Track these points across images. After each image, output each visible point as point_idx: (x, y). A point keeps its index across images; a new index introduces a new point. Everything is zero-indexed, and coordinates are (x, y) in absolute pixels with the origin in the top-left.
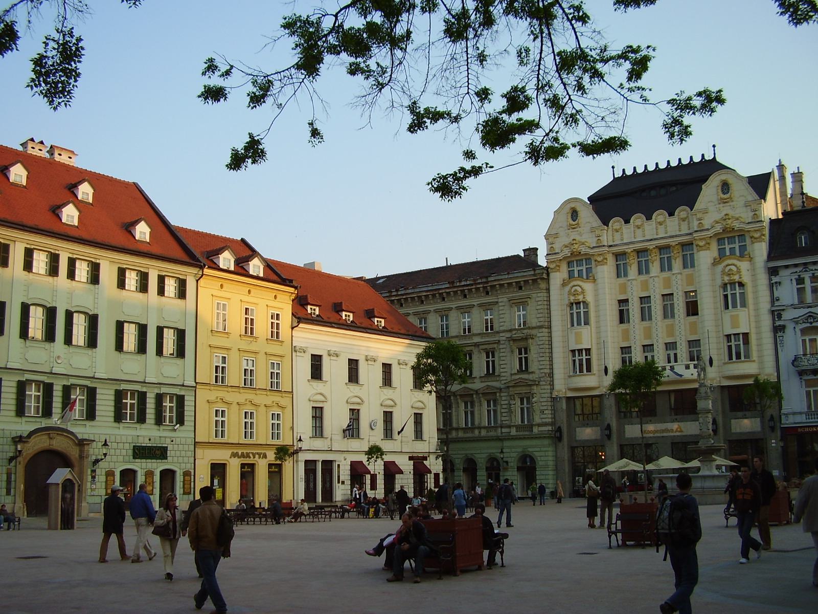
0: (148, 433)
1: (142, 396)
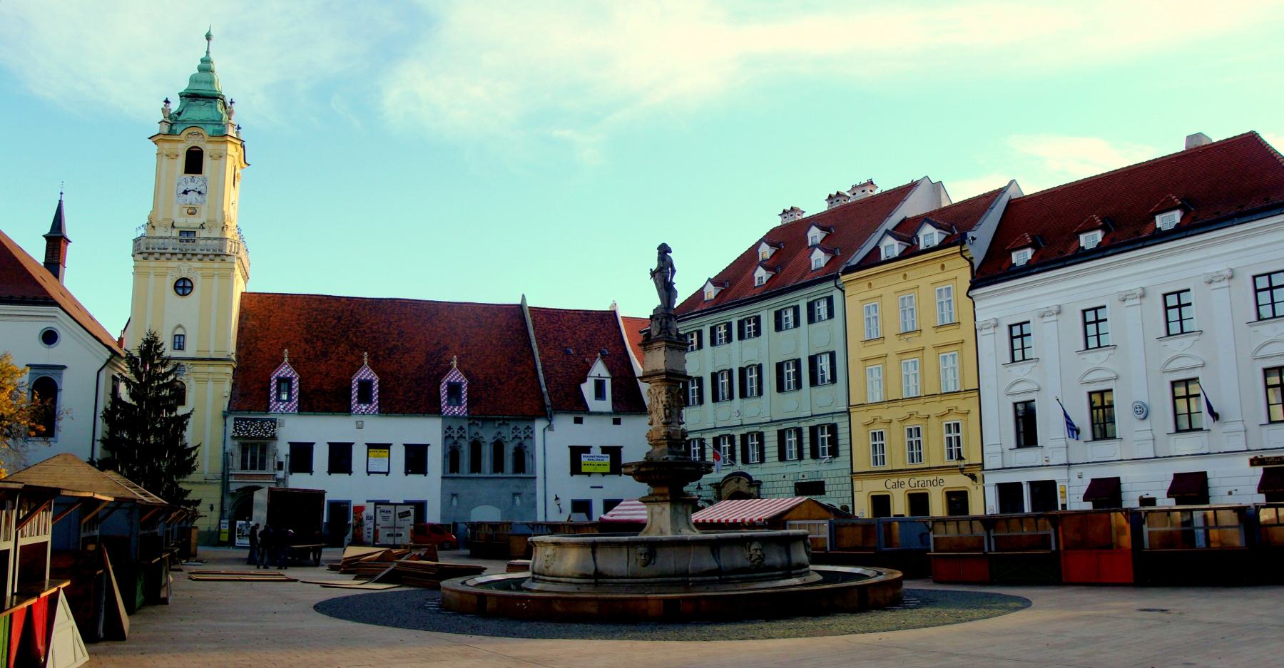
0: (808, 469)
1: (799, 431)
